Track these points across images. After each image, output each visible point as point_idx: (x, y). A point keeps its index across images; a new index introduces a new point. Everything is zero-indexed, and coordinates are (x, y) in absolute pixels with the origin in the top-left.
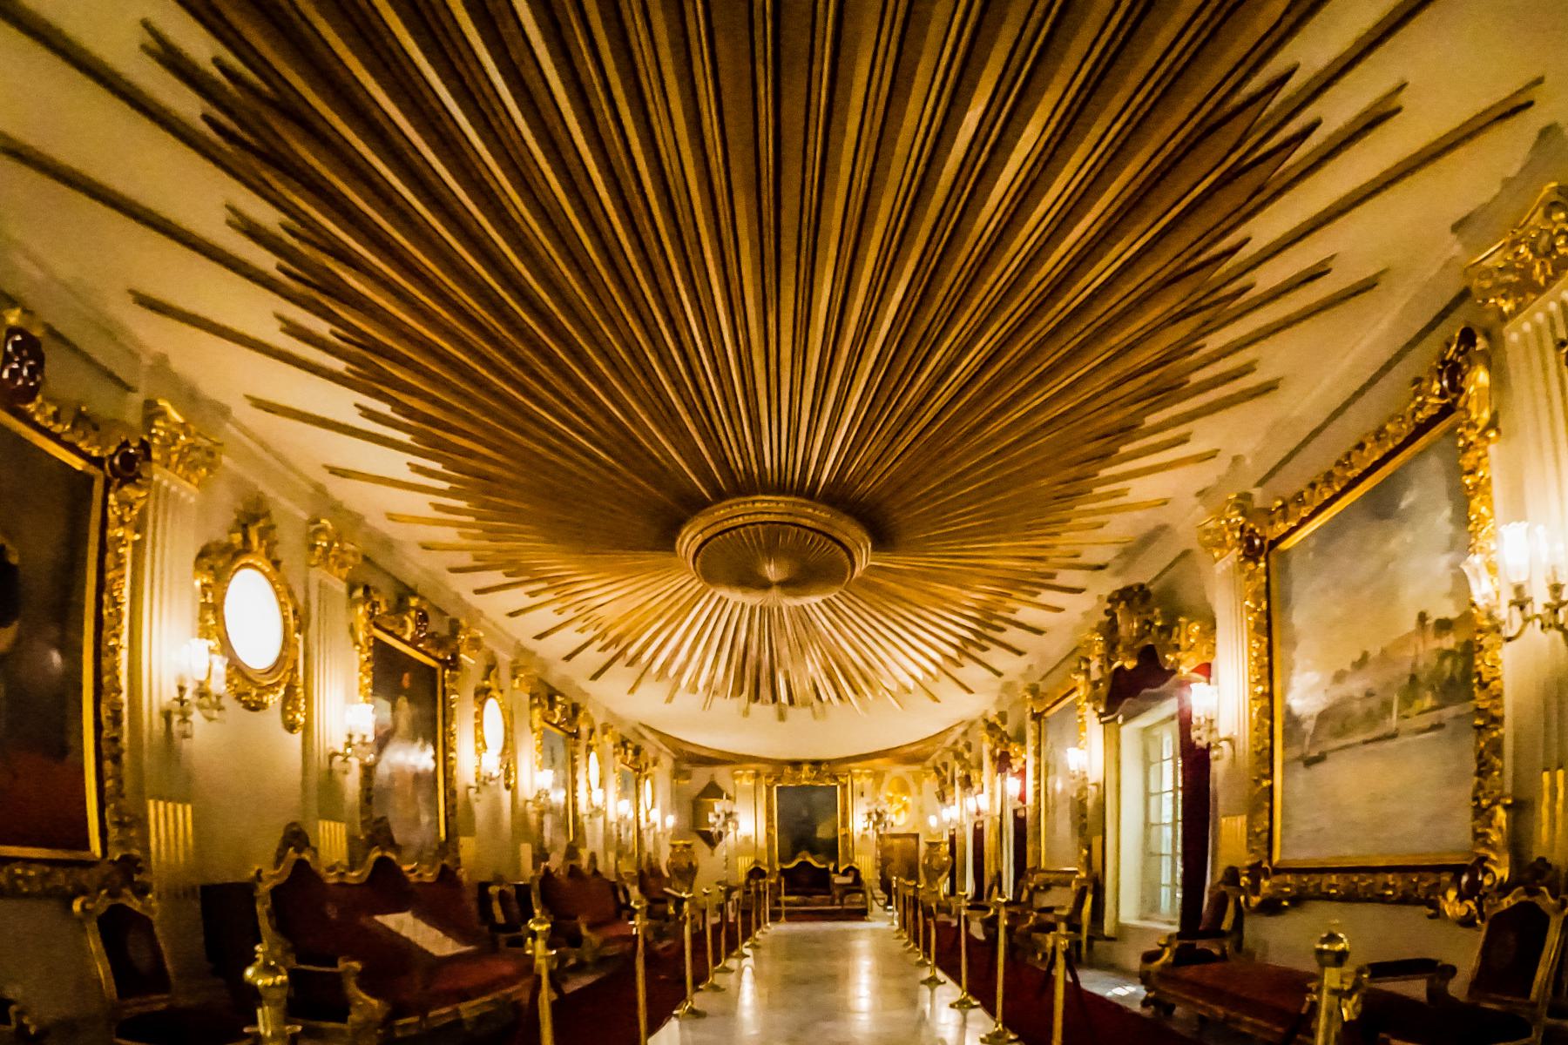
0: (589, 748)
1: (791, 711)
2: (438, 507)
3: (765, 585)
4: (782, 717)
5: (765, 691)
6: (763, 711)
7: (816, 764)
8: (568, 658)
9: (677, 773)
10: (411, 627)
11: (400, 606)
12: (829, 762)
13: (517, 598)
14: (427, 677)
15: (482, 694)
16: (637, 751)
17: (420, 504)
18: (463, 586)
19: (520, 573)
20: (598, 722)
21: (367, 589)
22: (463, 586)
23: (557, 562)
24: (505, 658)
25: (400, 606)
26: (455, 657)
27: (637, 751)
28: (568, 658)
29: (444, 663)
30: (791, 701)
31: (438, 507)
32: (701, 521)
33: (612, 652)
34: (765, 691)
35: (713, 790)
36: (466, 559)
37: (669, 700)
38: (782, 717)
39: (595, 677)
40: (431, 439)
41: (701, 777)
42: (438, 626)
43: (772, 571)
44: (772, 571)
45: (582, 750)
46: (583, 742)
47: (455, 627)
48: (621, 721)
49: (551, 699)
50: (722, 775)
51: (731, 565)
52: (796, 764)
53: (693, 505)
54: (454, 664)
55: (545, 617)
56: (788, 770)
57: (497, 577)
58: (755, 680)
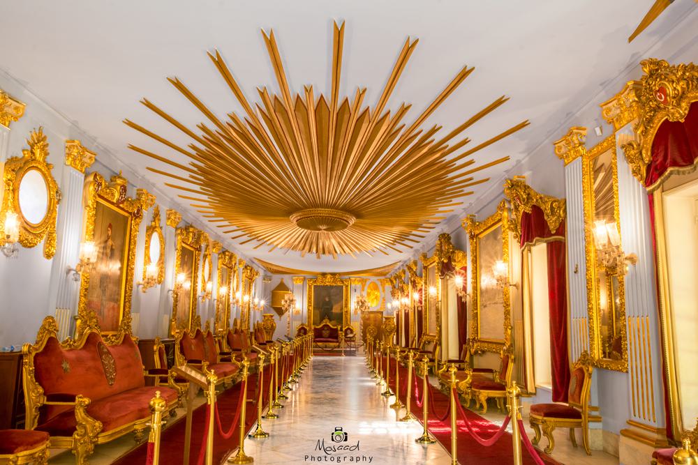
1: (323, 256)
4: (319, 257)
7: (333, 274)
12: (340, 274)
27: (251, 270)
35: (282, 287)
38: (319, 257)
52: (324, 274)
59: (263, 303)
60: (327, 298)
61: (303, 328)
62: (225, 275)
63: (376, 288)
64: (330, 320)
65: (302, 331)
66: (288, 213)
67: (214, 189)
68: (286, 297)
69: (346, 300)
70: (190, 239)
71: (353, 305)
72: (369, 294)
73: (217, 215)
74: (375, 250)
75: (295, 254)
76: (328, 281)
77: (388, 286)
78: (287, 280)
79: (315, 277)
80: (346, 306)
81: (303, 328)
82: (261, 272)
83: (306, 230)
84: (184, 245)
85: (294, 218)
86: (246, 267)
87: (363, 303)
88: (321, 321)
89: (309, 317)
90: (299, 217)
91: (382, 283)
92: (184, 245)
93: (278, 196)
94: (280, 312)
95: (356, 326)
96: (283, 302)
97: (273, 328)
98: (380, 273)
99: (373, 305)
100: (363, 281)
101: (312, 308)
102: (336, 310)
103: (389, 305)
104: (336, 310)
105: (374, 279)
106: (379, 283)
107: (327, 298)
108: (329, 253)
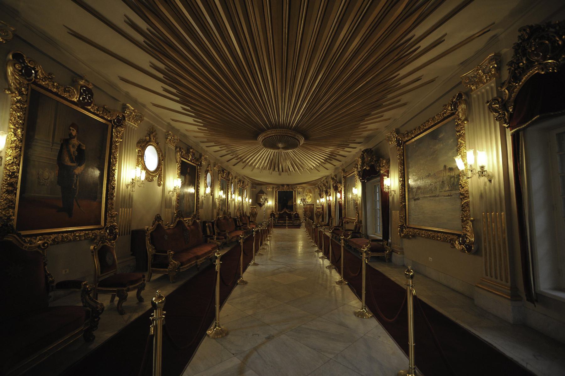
0: (232, 183)
1: (282, 173)
2: (199, 129)
3: (279, 148)
4: (280, 174)
5: (277, 169)
6: (276, 173)
7: (288, 185)
8: (228, 161)
9: (253, 187)
10: (190, 157)
11: (188, 152)
12: (291, 185)
13: (217, 148)
14: (193, 168)
15: (207, 172)
16: (243, 182)
17: (195, 128)
18: (203, 145)
19: (217, 143)
20: (234, 175)
21: (180, 149)
22: (203, 145)
23: (226, 141)
24: (212, 162)
25: (188, 152)
26: (201, 163)
27: (243, 182)
28: (228, 161)
29: (198, 165)
30: (283, 171)
31: (199, 129)
32: (264, 134)
33: (239, 160)
34: (277, 169)
35: (262, 192)
36: (205, 140)
37: (252, 171)
38: (280, 174)
39: (234, 165)
40: (198, 115)
41: (259, 188)
42: (197, 156)
43: (280, 145)
44: (280, 145)
45: (230, 184)
46: (230, 182)
47: (201, 156)
48: (239, 175)
49: (223, 171)
50: (263, 188)
51: (270, 144)
52: (283, 185)
53: (263, 131)
54: (201, 165)
55: (224, 152)
56: (281, 187)
57: (213, 144)
58: (274, 165)
59: (250, 201)
60: (285, 198)
61: (273, 213)
62: (225, 184)
63: (310, 192)
64: (287, 209)
65: (272, 215)
66: (255, 137)
67: (191, 108)
68: (263, 197)
69: (295, 198)
70: (190, 157)
71: (299, 201)
72: (307, 195)
73: (208, 141)
74: (313, 168)
75: (266, 172)
76: (285, 189)
77: (317, 190)
78: (263, 188)
79: (278, 186)
80: (295, 201)
81: (273, 213)
82: (250, 185)
83: (272, 150)
84: (182, 159)
85: (260, 138)
86: (240, 181)
87: (304, 200)
88: (282, 210)
89: (276, 208)
90: (263, 138)
91: (314, 190)
92: (182, 159)
93: (244, 112)
94: (261, 205)
95: (300, 212)
96: (261, 200)
97: (256, 214)
98: (313, 184)
99: (309, 201)
100: (304, 188)
101: (277, 203)
102: (289, 203)
103: (318, 201)
104: (289, 203)
105: (309, 187)
106: (312, 190)
107: (285, 198)
108: (286, 171)
